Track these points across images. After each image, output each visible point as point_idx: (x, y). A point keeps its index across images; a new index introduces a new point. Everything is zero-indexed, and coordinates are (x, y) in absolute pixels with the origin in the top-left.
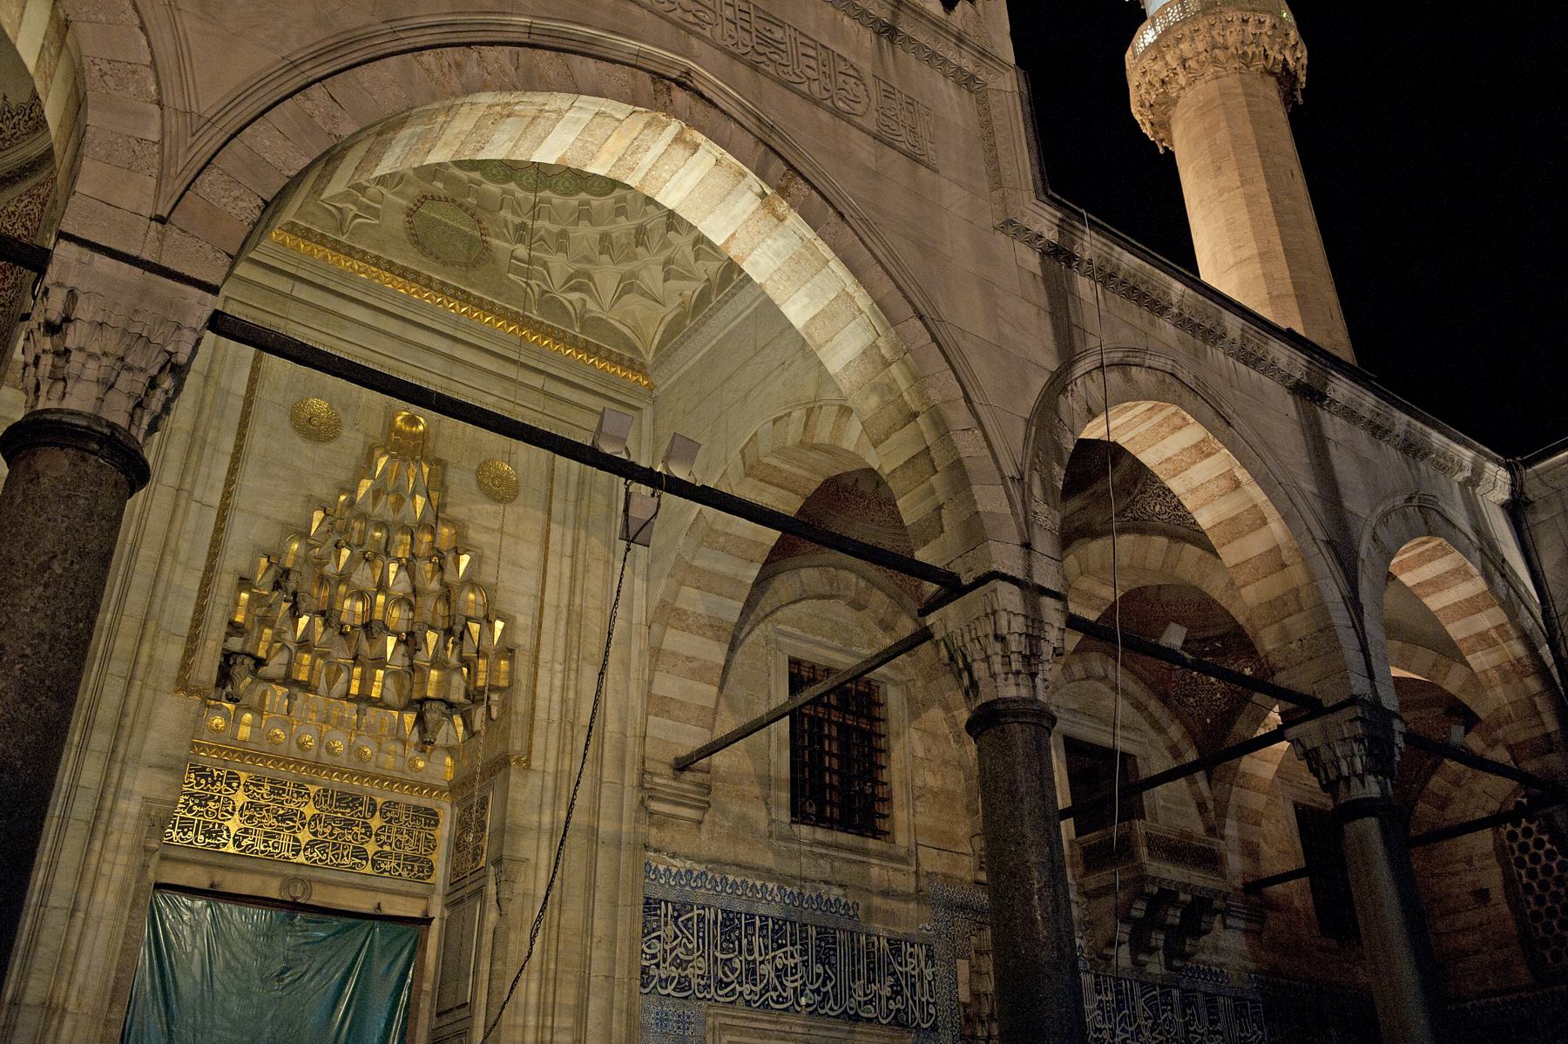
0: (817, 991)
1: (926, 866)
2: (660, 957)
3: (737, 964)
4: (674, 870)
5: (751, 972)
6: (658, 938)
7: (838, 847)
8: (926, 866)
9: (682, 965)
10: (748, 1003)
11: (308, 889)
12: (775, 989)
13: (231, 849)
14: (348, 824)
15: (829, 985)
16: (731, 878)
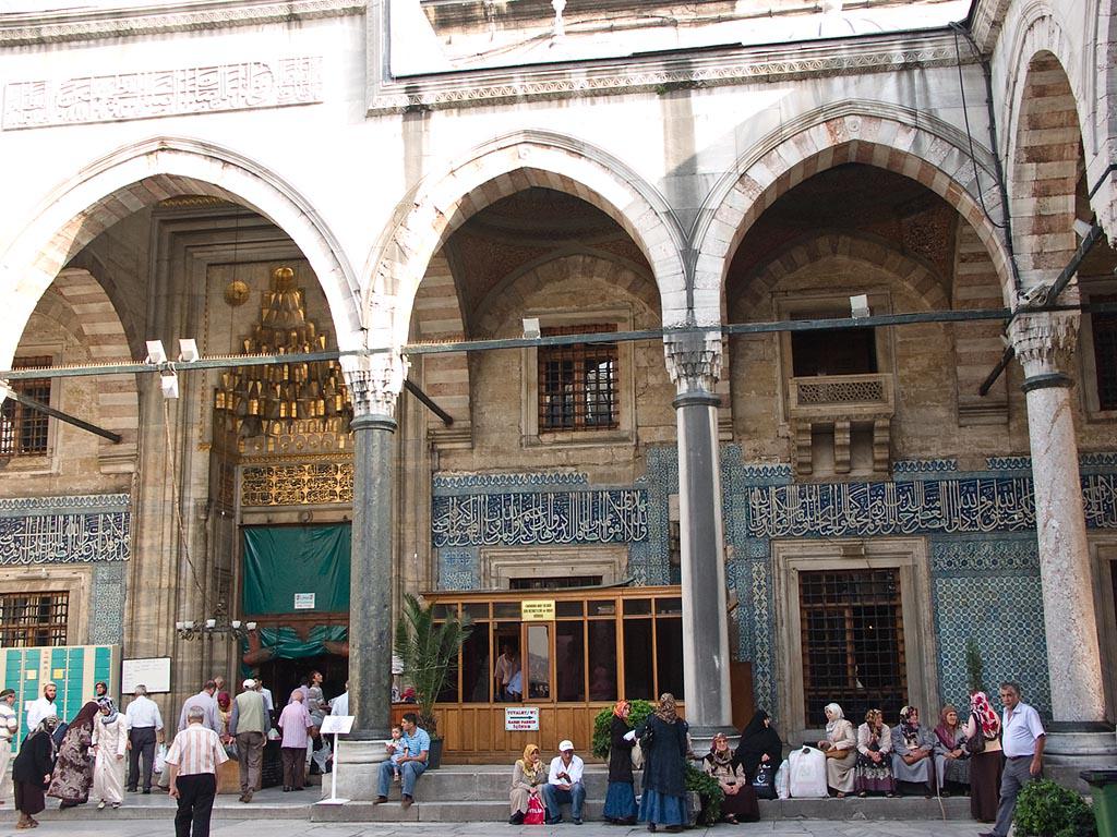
0: (555, 530)
1: (645, 439)
2: (449, 526)
3: (498, 523)
4: (457, 479)
5: (508, 526)
6: (448, 517)
7: (577, 442)
8: (645, 439)
9: (464, 528)
10: (506, 543)
11: (310, 515)
12: (525, 533)
13: (274, 503)
14: (326, 480)
15: (563, 526)
16: (493, 476)
